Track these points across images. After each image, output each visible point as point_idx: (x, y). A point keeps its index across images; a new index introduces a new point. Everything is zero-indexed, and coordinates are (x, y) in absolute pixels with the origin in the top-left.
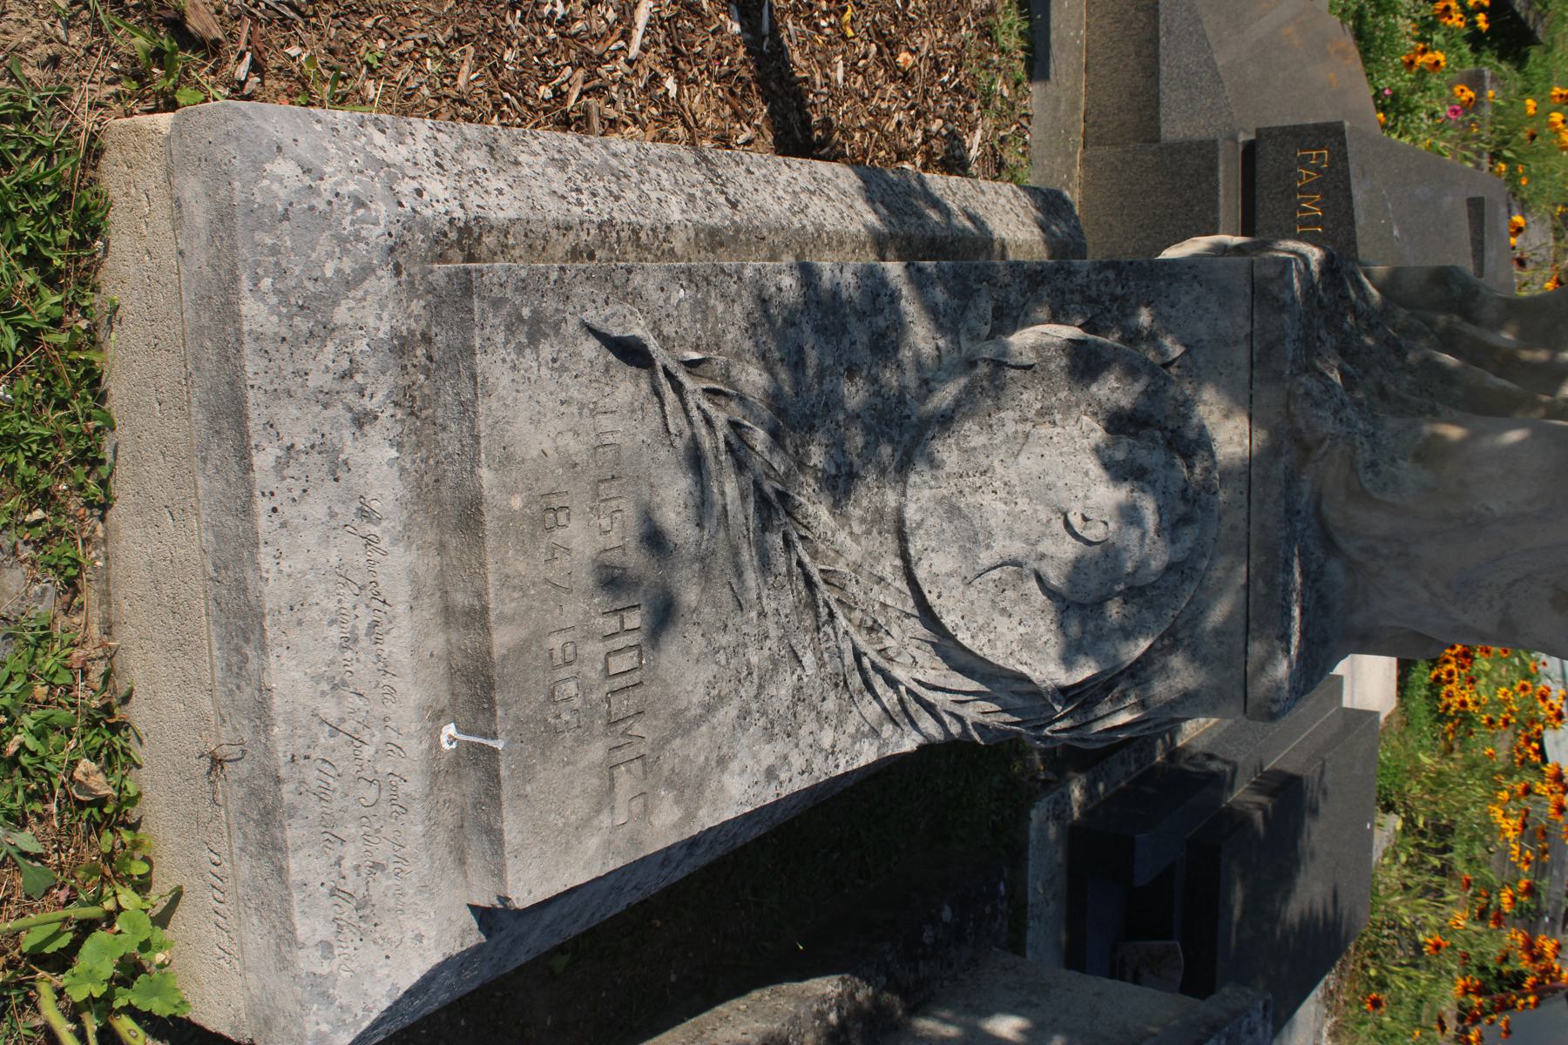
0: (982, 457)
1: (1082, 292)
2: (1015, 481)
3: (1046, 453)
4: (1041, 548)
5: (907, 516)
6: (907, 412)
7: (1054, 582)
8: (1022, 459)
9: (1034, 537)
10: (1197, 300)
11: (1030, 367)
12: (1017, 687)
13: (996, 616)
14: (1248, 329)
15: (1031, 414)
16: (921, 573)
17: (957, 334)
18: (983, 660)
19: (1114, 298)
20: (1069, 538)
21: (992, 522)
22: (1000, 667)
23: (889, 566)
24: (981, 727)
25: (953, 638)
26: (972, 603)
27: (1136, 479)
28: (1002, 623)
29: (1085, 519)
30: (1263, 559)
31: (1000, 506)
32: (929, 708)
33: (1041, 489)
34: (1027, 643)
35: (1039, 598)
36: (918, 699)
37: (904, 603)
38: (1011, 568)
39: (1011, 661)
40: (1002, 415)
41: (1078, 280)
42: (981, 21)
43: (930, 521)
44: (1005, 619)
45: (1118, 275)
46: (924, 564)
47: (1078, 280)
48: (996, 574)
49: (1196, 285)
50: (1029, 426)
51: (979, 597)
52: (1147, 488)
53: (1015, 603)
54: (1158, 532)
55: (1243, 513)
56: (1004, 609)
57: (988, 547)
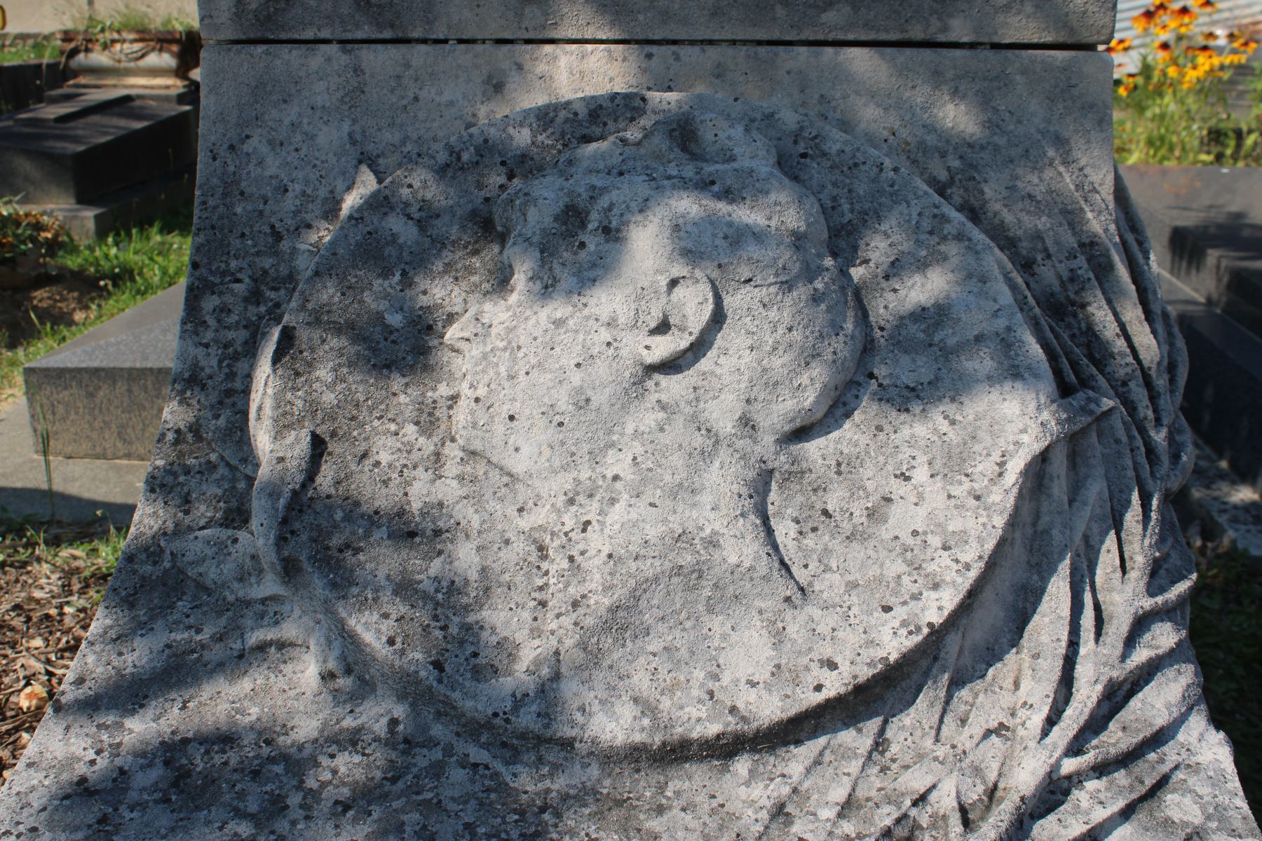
0: (509, 556)
1: (236, 357)
2: (564, 482)
3: (505, 410)
4: (726, 426)
5: (620, 739)
6: (380, 728)
7: (809, 398)
8: (519, 465)
9: (699, 440)
10: (276, 145)
11: (318, 445)
12: (1059, 489)
13: (885, 532)
14: (333, 49)
15: (427, 445)
16: (770, 708)
17: (248, 603)
18: (993, 563)
19: (255, 297)
20: (705, 364)
21: (652, 532)
22: (1013, 523)
23: (747, 789)
24: (1157, 577)
25: (938, 635)
26: (853, 585)
27: (583, 225)
28: (904, 518)
29: (663, 327)
30: (780, 12)
31: (617, 514)
32: (1116, 697)
33: (584, 424)
34: (953, 464)
35: (849, 436)
36: (1096, 724)
37: (847, 754)
38: (773, 496)
39: (995, 497)
40: (416, 506)
41: (210, 362)
42: (76, 586)
43: (641, 681)
44: (895, 511)
45: (210, 288)
46: (747, 699)
47: (210, 362)
48: (784, 531)
49: (247, 147)
50: (452, 452)
51: (834, 568)
52: (604, 202)
53: (857, 488)
54: (704, 185)
55: (690, 54)
56: (871, 514)
57: (712, 543)
